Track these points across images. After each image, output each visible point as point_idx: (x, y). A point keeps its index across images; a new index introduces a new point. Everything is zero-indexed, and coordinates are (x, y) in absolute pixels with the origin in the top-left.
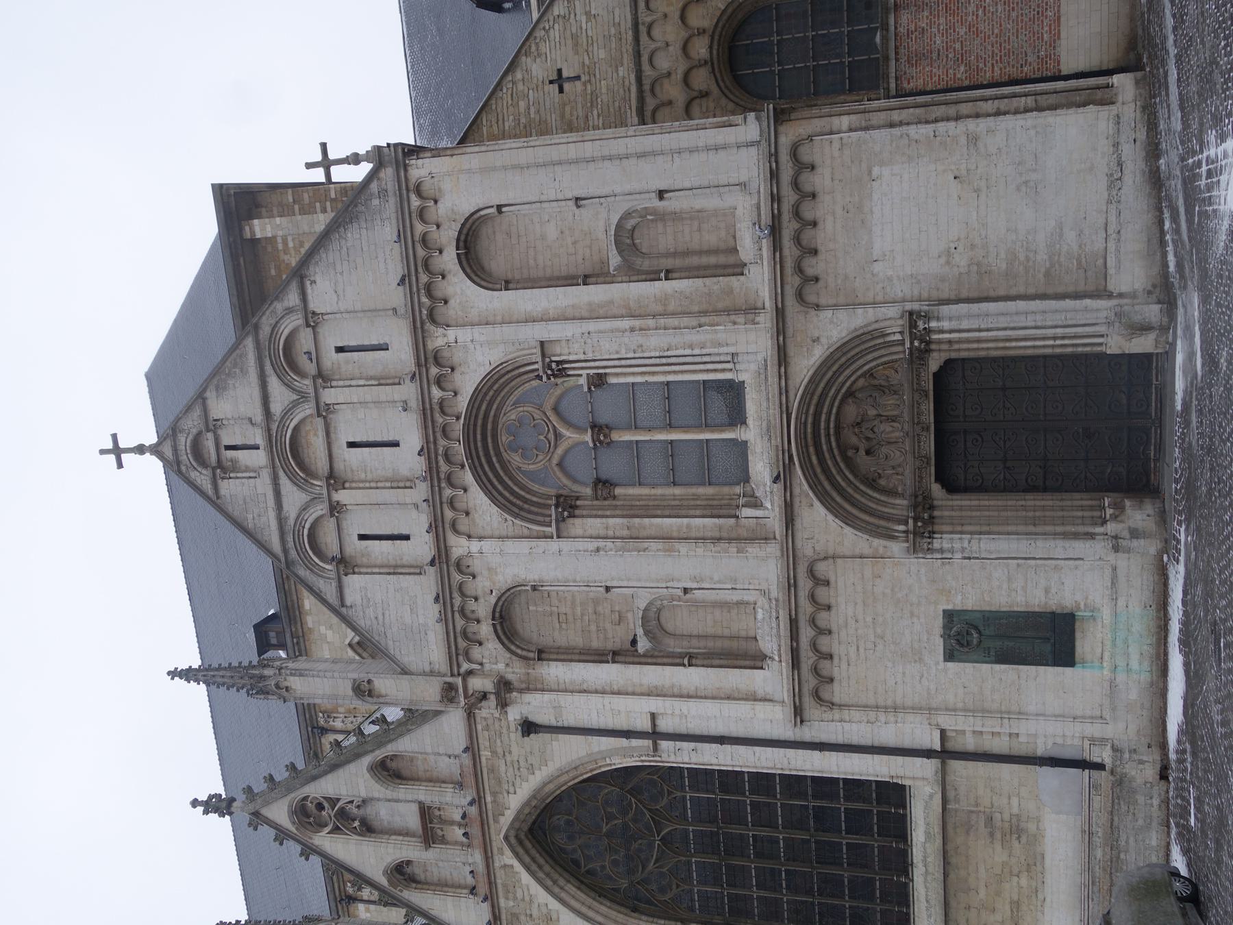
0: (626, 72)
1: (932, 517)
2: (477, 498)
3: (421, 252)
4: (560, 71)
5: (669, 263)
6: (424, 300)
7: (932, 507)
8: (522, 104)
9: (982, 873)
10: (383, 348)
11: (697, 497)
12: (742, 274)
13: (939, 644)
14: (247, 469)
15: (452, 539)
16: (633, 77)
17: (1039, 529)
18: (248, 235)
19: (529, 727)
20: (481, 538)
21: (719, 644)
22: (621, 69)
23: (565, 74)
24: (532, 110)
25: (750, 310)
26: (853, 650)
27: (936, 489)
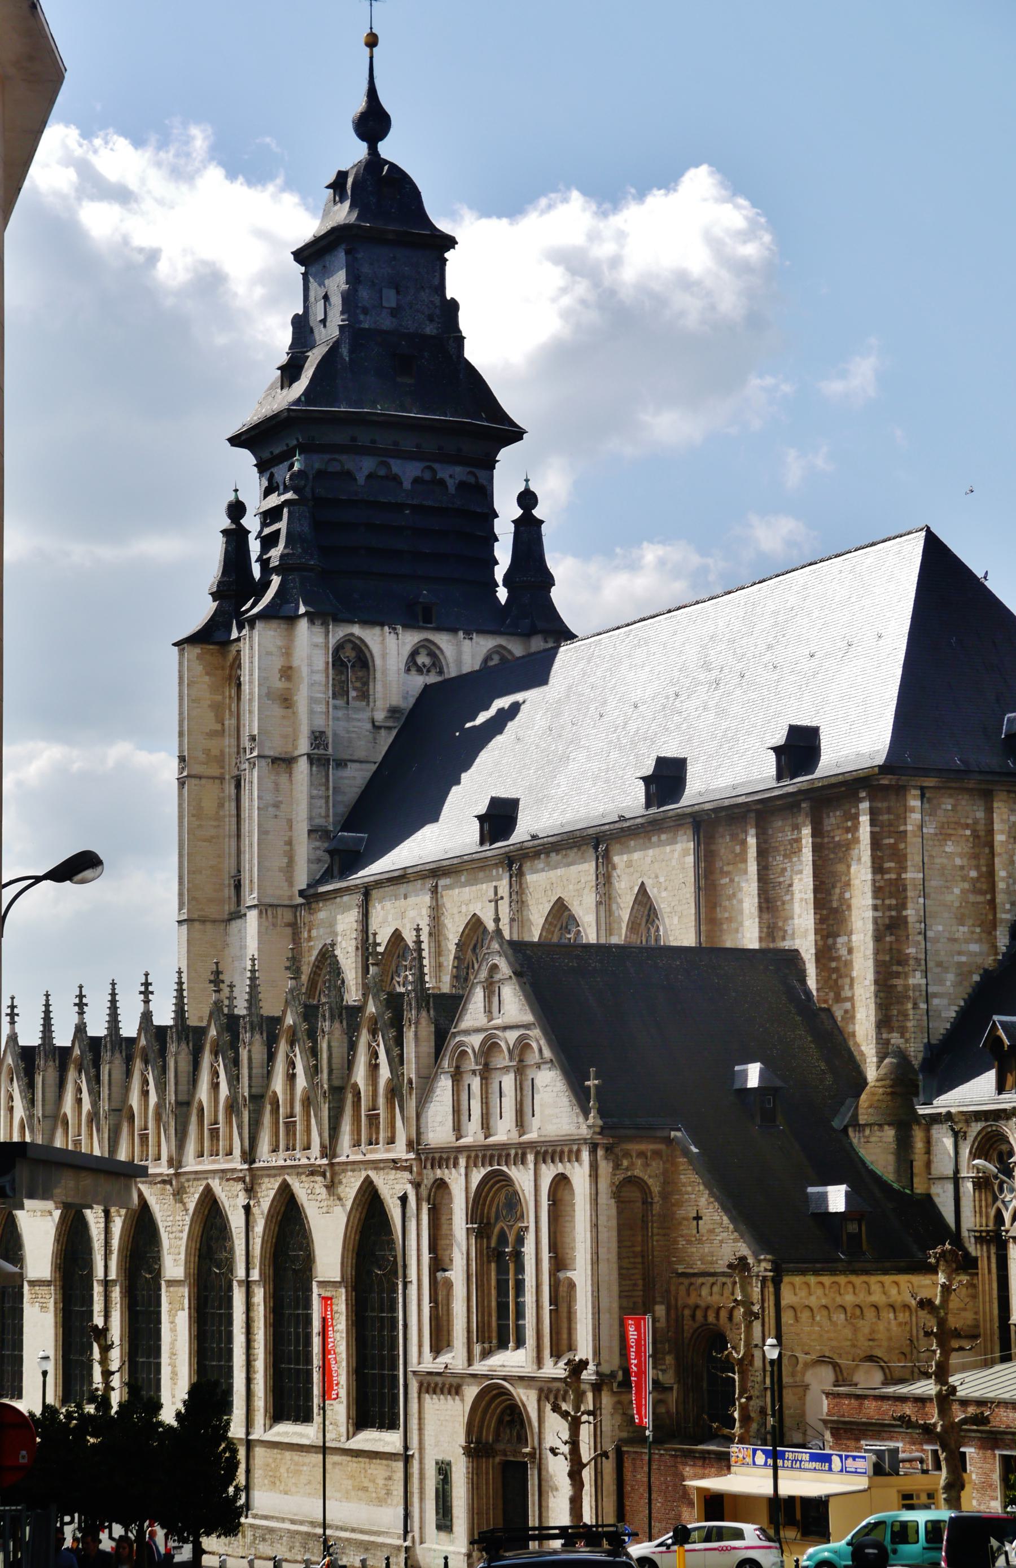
0: (699, 1266)
1: (482, 1457)
2: (483, 1172)
3: (559, 1149)
4: (701, 1218)
5: (563, 1309)
6: (543, 1149)
7: (488, 1457)
8: (689, 1189)
9: (375, 1472)
10: (533, 1116)
11: (490, 1315)
12: (551, 1356)
13: (440, 1458)
14: (490, 1002)
15: (465, 1154)
16: (696, 1271)
17: (475, 1516)
18: (863, 794)
19: (404, 1199)
20: (467, 1175)
21: (445, 1323)
22: (699, 1263)
23: (700, 1222)
24: (686, 1196)
25: (539, 1362)
26: (436, 1407)
27: (498, 1459)
